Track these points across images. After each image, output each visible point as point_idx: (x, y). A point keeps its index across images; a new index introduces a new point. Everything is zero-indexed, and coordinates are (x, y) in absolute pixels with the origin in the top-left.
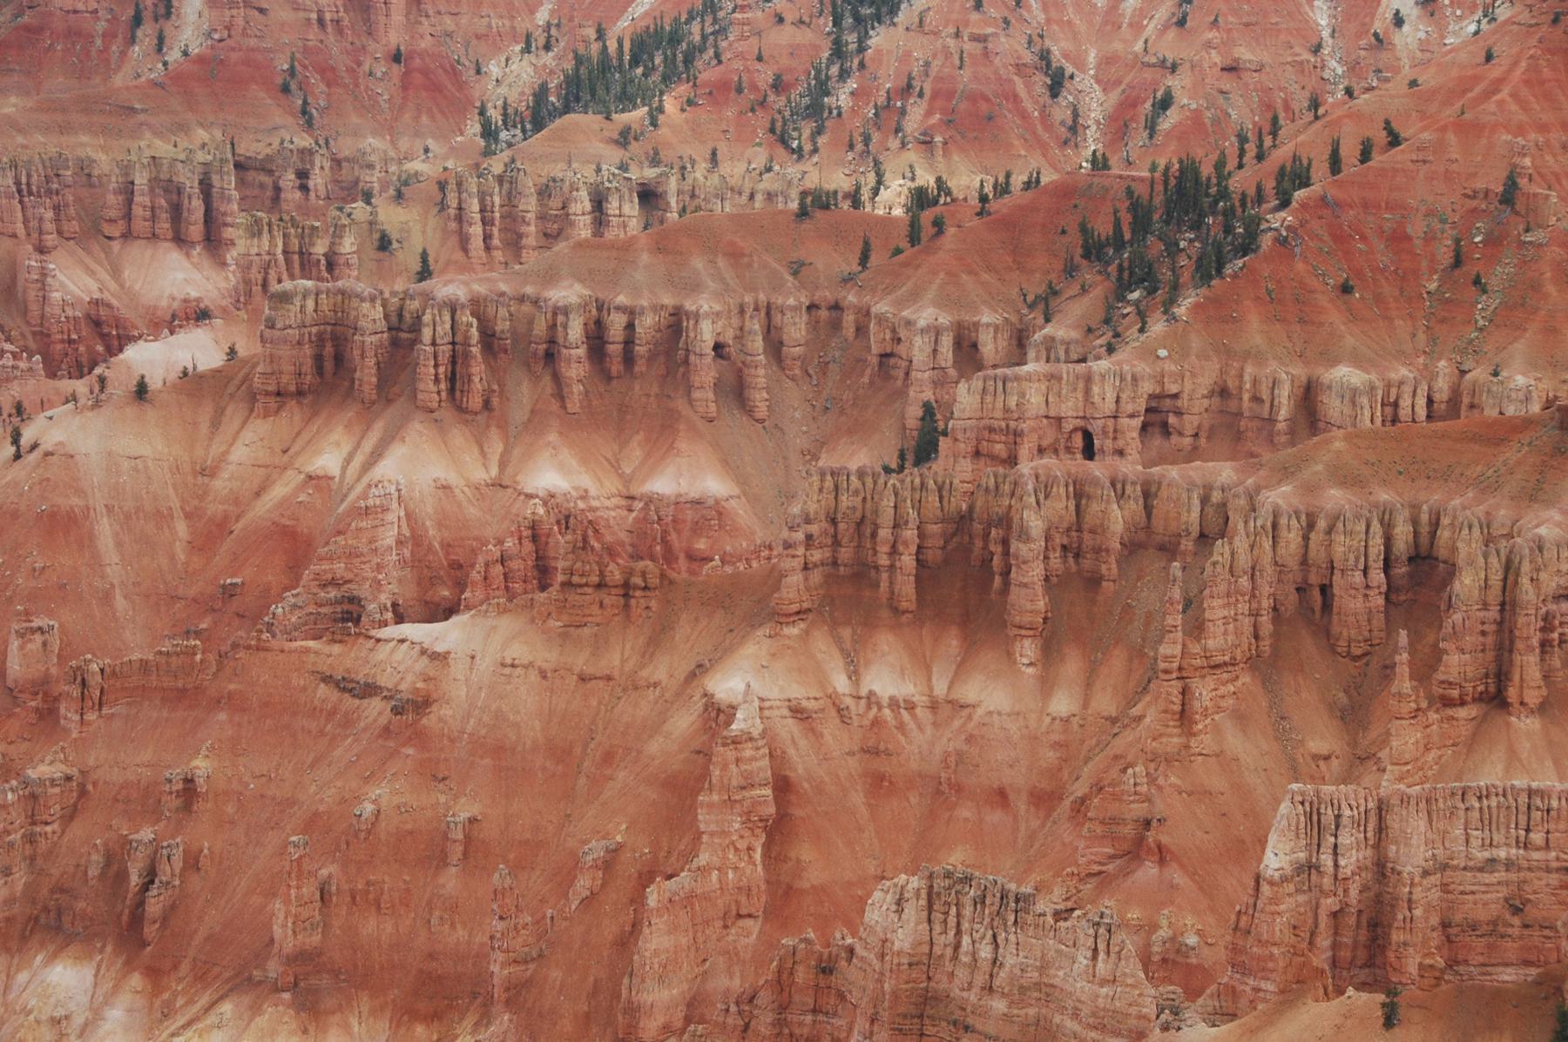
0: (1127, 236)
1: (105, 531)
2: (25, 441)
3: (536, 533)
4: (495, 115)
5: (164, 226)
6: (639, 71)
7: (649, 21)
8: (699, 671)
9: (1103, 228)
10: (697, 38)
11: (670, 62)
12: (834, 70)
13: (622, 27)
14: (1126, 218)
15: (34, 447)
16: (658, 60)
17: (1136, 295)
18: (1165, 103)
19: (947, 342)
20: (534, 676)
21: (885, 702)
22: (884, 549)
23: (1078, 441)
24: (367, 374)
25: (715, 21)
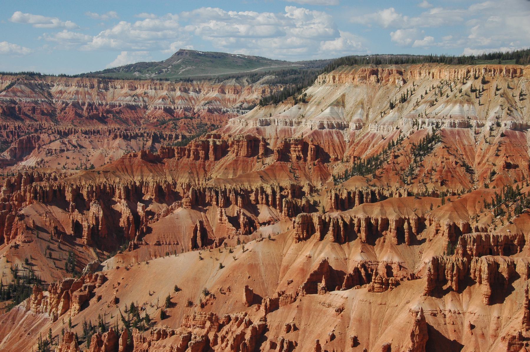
0: (496, 203)
1: (262, 269)
2: (245, 249)
3: (356, 270)
4: (337, 177)
5: (264, 201)
6: (369, 166)
7: (370, 155)
8: (408, 303)
9: (489, 201)
10: (382, 159)
11: (376, 165)
12: (415, 165)
13: (363, 157)
14: (495, 199)
15: (247, 250)
16: (373, 163)
17: (499, 217)
18: (494, 173)
19: (453, 229)
20: (368, 304)
21: (453, 312)
22: (449, 276)
23: (488, 251)
24: (318, 234)
25: (387, 155)
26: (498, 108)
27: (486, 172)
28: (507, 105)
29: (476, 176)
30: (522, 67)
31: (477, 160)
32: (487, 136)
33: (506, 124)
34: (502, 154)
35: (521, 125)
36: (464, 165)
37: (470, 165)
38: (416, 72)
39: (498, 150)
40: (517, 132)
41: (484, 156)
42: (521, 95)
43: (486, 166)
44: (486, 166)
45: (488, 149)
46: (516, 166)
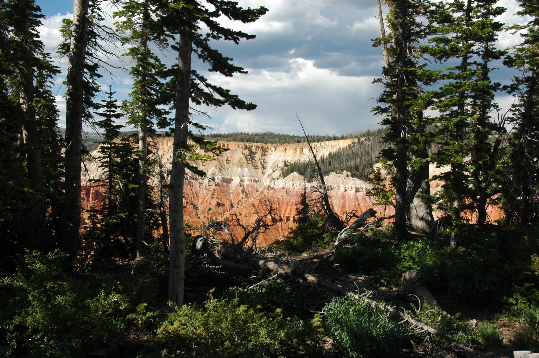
18: (210, 209)
26: (214, 168)
27: (205, 208)
28: (219, 166)
29: (199, 211)
30: (228, 143)
31: (200, 201)
32: (207, 186)
33: (218, 178)
34: (215, 197)
35: (227, 179)
36: (192, 204)
37: (196, 204)
38: (165, 143)
39: (213, 195)
40: (225, 183)
41: (204, 198)
42: (227, 160)
43: (206, 205)
44: (206, 205)
45: (207, 194)
46: (223, 205)
